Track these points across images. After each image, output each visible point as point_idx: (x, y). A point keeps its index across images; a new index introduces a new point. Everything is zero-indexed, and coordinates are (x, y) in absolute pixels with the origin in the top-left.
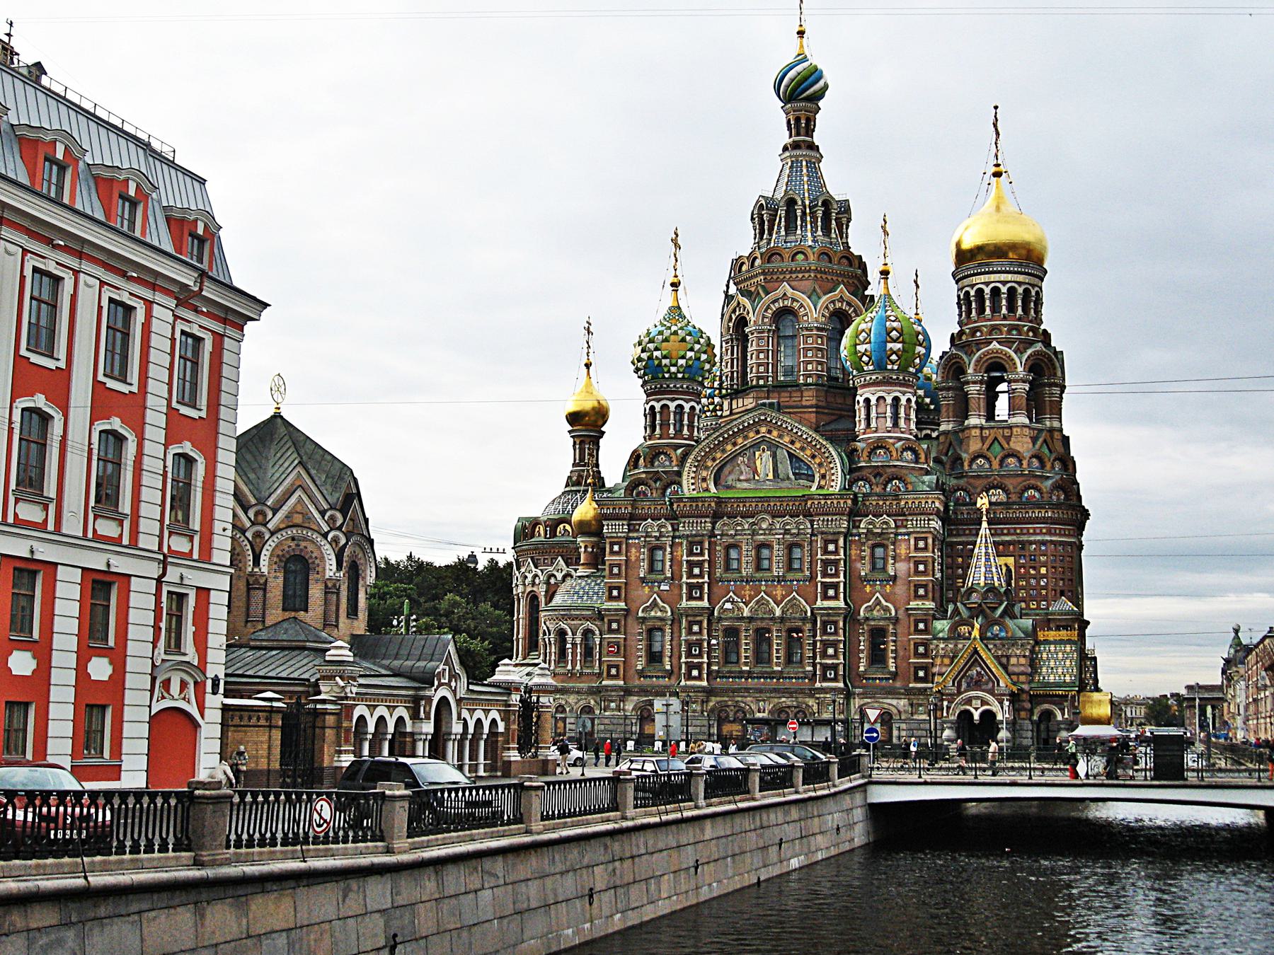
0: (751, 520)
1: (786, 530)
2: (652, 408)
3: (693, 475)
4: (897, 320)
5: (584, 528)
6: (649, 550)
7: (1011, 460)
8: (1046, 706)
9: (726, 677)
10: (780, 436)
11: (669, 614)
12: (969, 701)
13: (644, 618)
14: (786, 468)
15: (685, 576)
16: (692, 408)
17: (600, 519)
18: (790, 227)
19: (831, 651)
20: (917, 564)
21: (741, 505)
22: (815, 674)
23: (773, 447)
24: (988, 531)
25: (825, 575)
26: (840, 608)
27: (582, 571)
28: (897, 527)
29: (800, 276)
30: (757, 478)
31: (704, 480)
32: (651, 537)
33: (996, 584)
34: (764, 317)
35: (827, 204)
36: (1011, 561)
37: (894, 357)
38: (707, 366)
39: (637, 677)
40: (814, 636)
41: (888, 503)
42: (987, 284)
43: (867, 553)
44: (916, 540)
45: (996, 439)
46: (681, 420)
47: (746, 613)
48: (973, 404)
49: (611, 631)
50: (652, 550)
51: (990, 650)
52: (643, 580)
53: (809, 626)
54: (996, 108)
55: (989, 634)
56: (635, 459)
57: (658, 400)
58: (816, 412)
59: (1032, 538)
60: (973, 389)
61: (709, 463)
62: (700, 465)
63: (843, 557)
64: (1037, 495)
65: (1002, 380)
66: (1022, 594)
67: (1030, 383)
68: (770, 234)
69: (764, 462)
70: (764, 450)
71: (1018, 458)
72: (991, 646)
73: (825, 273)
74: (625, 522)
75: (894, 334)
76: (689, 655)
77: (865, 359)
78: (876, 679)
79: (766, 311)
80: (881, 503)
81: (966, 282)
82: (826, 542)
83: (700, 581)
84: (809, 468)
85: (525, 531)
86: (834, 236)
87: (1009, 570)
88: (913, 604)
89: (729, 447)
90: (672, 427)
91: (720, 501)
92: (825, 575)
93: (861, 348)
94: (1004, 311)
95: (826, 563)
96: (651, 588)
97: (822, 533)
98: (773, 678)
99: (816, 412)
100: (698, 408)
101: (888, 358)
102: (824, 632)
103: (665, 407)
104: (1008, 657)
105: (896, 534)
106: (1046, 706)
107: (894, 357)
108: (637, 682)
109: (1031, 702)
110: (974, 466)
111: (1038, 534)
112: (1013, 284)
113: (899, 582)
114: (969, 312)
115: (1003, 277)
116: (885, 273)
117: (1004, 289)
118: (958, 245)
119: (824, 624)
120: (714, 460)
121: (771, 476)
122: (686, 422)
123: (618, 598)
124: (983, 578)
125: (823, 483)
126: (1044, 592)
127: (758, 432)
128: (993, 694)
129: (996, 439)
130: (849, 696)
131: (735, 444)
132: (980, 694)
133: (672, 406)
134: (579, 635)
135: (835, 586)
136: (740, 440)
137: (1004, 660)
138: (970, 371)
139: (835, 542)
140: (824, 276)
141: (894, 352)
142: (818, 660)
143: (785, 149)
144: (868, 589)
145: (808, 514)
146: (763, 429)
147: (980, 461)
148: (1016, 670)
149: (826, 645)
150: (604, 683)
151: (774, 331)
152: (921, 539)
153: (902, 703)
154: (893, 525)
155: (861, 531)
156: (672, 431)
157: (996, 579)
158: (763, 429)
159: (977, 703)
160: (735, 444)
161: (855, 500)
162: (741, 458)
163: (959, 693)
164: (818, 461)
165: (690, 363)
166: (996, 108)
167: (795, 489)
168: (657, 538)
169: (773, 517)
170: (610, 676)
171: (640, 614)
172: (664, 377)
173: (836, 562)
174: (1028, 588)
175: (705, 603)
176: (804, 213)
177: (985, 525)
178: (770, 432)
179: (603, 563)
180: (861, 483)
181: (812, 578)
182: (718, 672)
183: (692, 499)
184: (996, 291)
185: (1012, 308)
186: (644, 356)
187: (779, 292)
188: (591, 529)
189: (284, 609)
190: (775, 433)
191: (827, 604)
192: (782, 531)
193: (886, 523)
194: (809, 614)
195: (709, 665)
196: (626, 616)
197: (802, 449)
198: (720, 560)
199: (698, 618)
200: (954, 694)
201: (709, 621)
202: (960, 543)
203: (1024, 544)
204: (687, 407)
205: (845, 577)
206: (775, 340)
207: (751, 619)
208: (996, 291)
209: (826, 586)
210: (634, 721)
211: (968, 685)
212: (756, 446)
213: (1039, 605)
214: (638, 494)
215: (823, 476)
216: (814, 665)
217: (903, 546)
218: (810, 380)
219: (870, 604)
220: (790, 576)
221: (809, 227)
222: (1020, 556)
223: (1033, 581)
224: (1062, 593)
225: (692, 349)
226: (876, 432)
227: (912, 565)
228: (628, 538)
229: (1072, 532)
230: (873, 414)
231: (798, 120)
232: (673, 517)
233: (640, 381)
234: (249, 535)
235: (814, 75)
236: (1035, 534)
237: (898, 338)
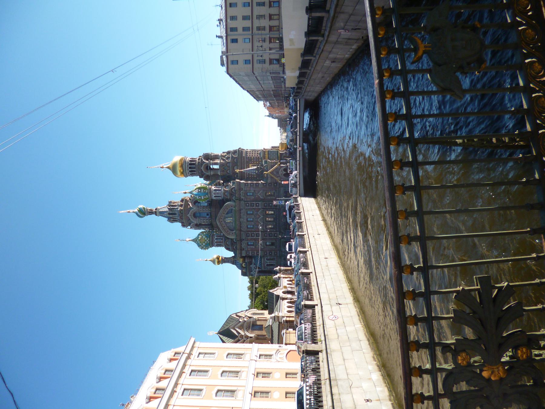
2: (216, 245)
5: (244, 261)
7: (228, 165)
14: (230, 215)
16: (216, 236)
17: (242, 257)
18: (175, 214)
23: (225, 218)
25: (254, 206)
26: (261, 204)
27: (253, 261)
36: (250, 165)
38: (207, 233)
42: (188, 170)
44: (246, 186)
45: (223, 168)
46: (219, 239)
49: (266, 254)
50: (248, 245)
52: (255, 247)
56: (228, 249)
57: (214, 244)
60: (212, 173)
61: (229, 232)
62: (229, 234)
65: (210, 167)
66: (258, 162)
68: (176, 219)
69: (229, 220)
76: (272, 236)
82: (246, 206)
85: (244, 274)
89: (225, 228)
92: (254, 206)
93: (203, 198)
94: (194, 166)
95: (251, 206)
100: (216, 235)
103: (216, 242)
107: (205, 191)
114: (195, 174)
115: (187, 166)
116: (185, 193)
117: (189, 166)
120: (228, 231)
121: (231, 218)
122: (219, 238)
127: (222, 221)
131: (224, 226)
133: (216, 241)
134: (267, 261)
135: (256, 204)
138: (208, 174)
139: (246, 204)
143: (156, 215)
144: (257, 197)
145: (240, 210)
146: (221, 220)
149: (269, 206)
156: (221, 241)
160: (224, 226)
161: (237, 199)
163: (280, 176)
168: (246, 244)
170: (277, 254)
173: (251, 204)
174: (256, 161)
176: (172, 211)
177: (242, 170)
178: (222, 219)
179: (251, 256)
180: (233, 198)
181: (254, 209)
184: (190, 168)
185: (194, 164)
186: (204, 247)
188: (244, 258)
189: (262, 330)
190: (222, 217)
197: (226, 211)
202: (246, 176)
203: (247, 162)
204: (216, 237)
208: (190, 168)
209: (256, 206)
212: (225, 222)
214: (236, 248)
215: (232, 207)
216: (274, 208)
217: (247, 189)
218: (210, 210)
230: (218, 195)
232: (241, 240)
233: (210, 248)
234: (245, 339)
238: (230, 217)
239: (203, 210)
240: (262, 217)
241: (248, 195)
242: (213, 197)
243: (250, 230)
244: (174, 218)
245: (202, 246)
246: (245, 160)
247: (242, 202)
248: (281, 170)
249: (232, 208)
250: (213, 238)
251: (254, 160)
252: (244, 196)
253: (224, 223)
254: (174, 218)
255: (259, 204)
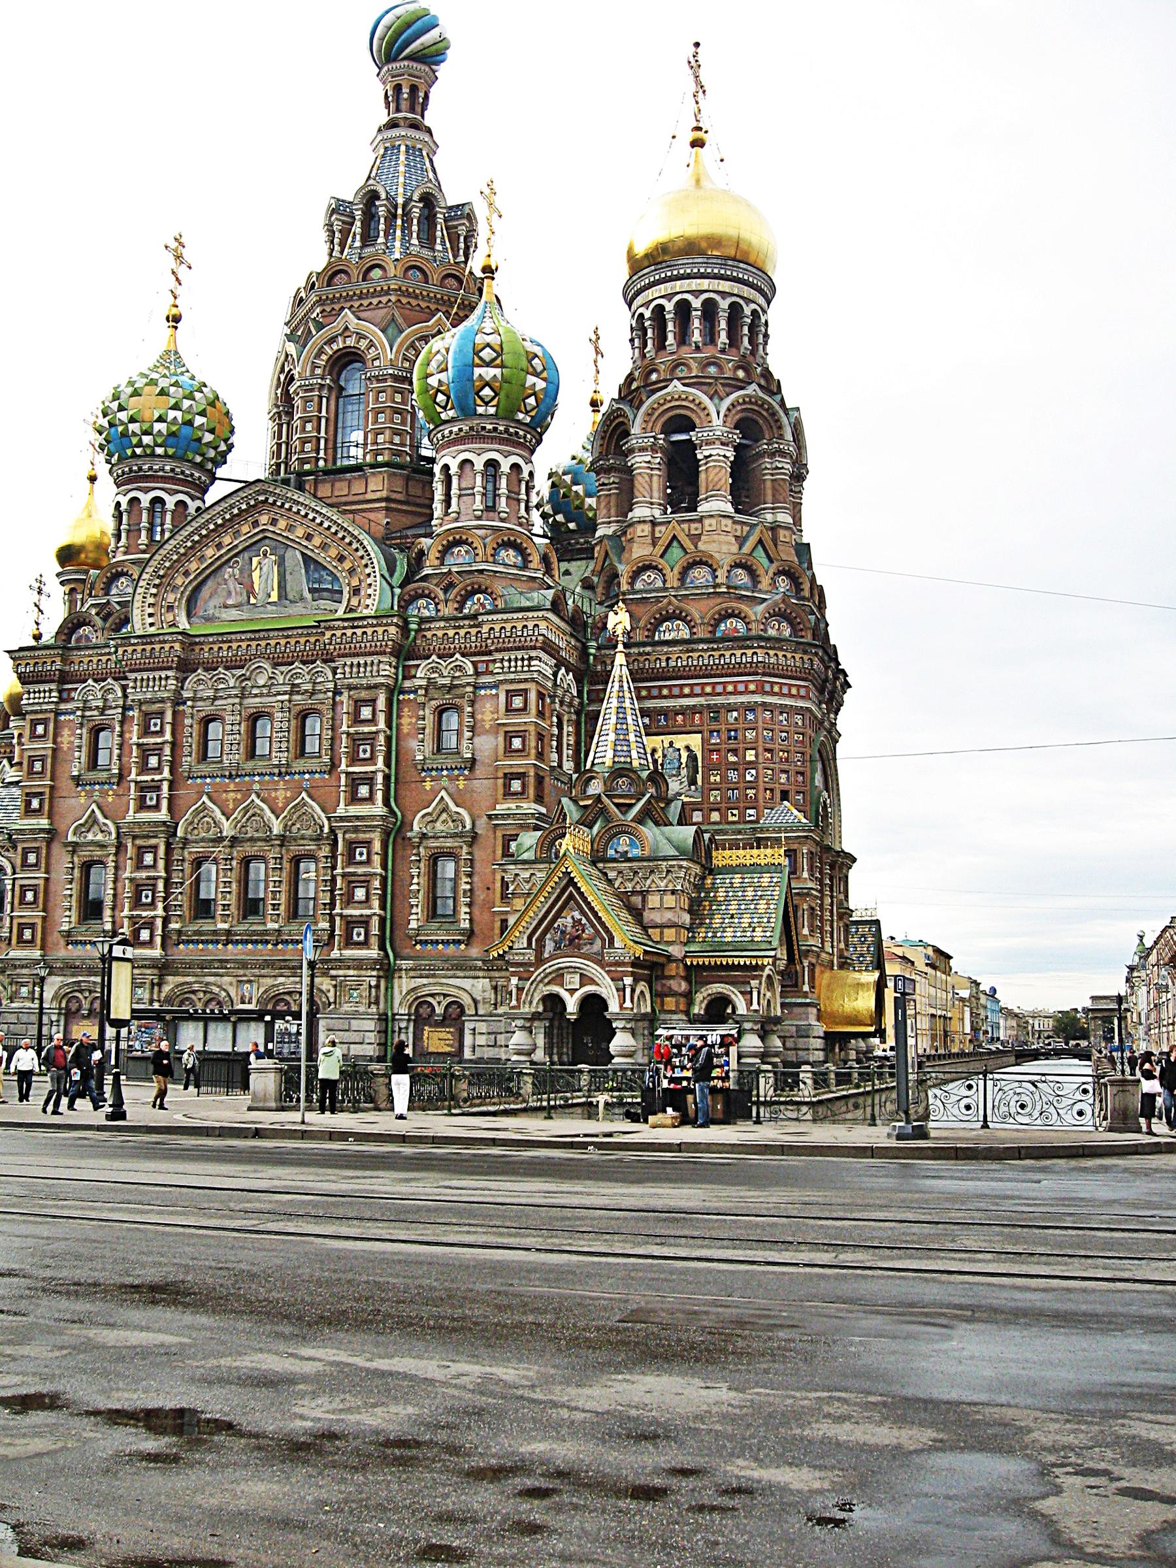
0: (239, 672)
1: (293, 685)
3: (151, 600)
4: (496, 332)
6: (91, 731)
8: (717, 988)
9: (192, 942)
10: (290, 528)
11: (114, 836)
12: (558, 977)
13: (75, 845)
14: (299, 581)
15: (134, 770)
18: (368, 238)
19: (360, 894)
20: (509, 736)
21: (225, 646)
22: (332, 935)
23: (281, 547)
24: (624, 668)
25: (354, 760)
28: (477, 674)
29: (375, 301)
30: (253, 601)
31: (170, 608)
32: (90, 709)
33: (636, 764)
34: (314, 366)
35: (429, 201)
36: (695, 741)
37: (487, 392)
39: (62, 942)
40: (334, 868)
41: (462, 632)
42: (669, 297)
43: (429, 721)
45: (674, 537)
47: (228, 829)
48: (640, 483)
50: (96, 731)
51: (610, 882)
52: (77, 780)
53: (325, 851)
54: (697, 45)
55: (611, 852)
58: (387, 509)
59: (732, 699)
63: (382, 725)
64: (740, 626)
67: (736, 449)
70: (265, 555)
71: (710, 566)
72: (612, 875)
73: (416, 297)
74: (53, 686)
75: (487, 354)
76: (137, 903)
77: (441, 398)
78: (437, 942)
79: (318, 356)
80: (451, 633)
81: (640, 300)
82: (358, 704)
83: (157, 777)
84: (336, 579)
86: (439, 247)
87: (692, 757)
88: (501, 808)
90: (144, 533)
91: (189, 641)
92: (354, 760)
94: (697, 337)
96: (89, 795)
97: (350, 688)
98: (267, 942)
99: (387, 509)
100: (193, 505)
101: (477, 394)
102: (350, 860)
104: (644, 894)
105: (476, 687)
106: (717, 988)
107: (487, 392)
108: (63, 952)
109: (687, 979)
110: (639, 585)
111: (741, 693)
112: (712, 295)
113: (480, 771)
115: (694, 284)
117: (696, 303)
118: (630, 251)
119: (351, 846)
121: (274, 597)
123: (38, 812)
124: (610, 754)
125: (354, 602)
126: (751, 792)
127: (256, 524)
128: (601, 963)
129: (674, 537)
130: (388, 972)
131: (219, 546)
132: (577, 962)
135: (369, 780)
136: (227, 540)
137: (637, 900)
138: (635, 430)
140: (414, 302)
141: (487, 384)
142: (337, 910)
144: (428, 785)
147: (648, 576)
148: (657, 918)
150: (12, 954)
151: (330, 388)
152: (518, 692)
153: (480, 987)
154: (471, 671)
155: (418, 682)
157: (634, 754)
158: (264, 519)
159: (573, 980)
162: (230, 570)
163: (540, 961)
164: (347, 565)
165: (174, 428)
166: (697, 45)
167: (306, 613)
169: (275, 665)
171: (71, 838)
172: (134, 455)
175: (163, 815)
178: (274, 522)
181: (334, 765)
182: (179, 932)
183: (146, 638)
184: (683, 309)
185: (711, 336)
187: (337, 325)
190: (282, 524)
191: (355, 810)
192: (288, 688)
193: (459, 668)
194: (326, 830)
195: (166, 921)
196: (49, 842)
198: (190, 742)
199: (153, 841)
200: (531, 965)
201: (168, 845)
203: (716, 711)
204: (171, 501)
205: (387, 764)
206: (333, 403)
207: (234, 841)
208: (683, 309)
209: (354, 781)
210: (54, 1018)
211: (557, 948)
213: (742, 815)
219: (429, 810)
220: (298, 766)
221: (398, 233)
222: (711, 732)
223: (733, 775)
224: (785, 796)
225: (176, 407)
226: (456, 520)
227: (501, 739)
228: (58, 713)
229: (803, 692)
230: (454, 491)
231: (398, 88)
235: (421, 23)
236: (735, 692)
237: (495, 359)
238: (282, 586)
239: (377, 412)
240: (277, 828)
241: (440, 712)
242: (446, 460)
243: (190, 742)
244: (345, 233)
245: (115, 405)
246: (732, 699)
247: (386, 670)
248: (593, 970)
249: (346, 596)
250: (164, 479)
251: (734, 767)
252: (431, 684)
253: (241, 541)
254: (345, 233)
255: (370, 799)
